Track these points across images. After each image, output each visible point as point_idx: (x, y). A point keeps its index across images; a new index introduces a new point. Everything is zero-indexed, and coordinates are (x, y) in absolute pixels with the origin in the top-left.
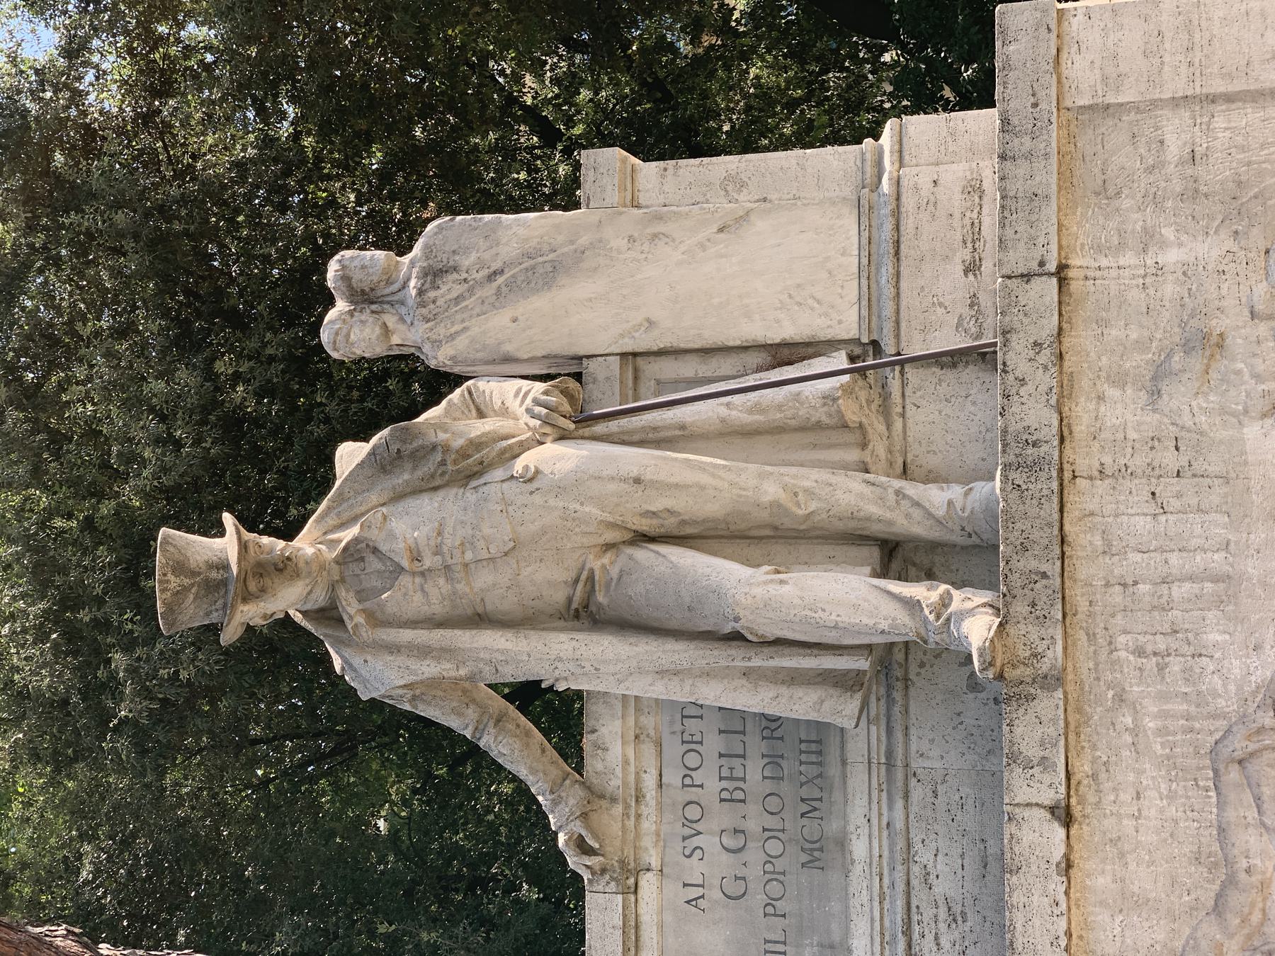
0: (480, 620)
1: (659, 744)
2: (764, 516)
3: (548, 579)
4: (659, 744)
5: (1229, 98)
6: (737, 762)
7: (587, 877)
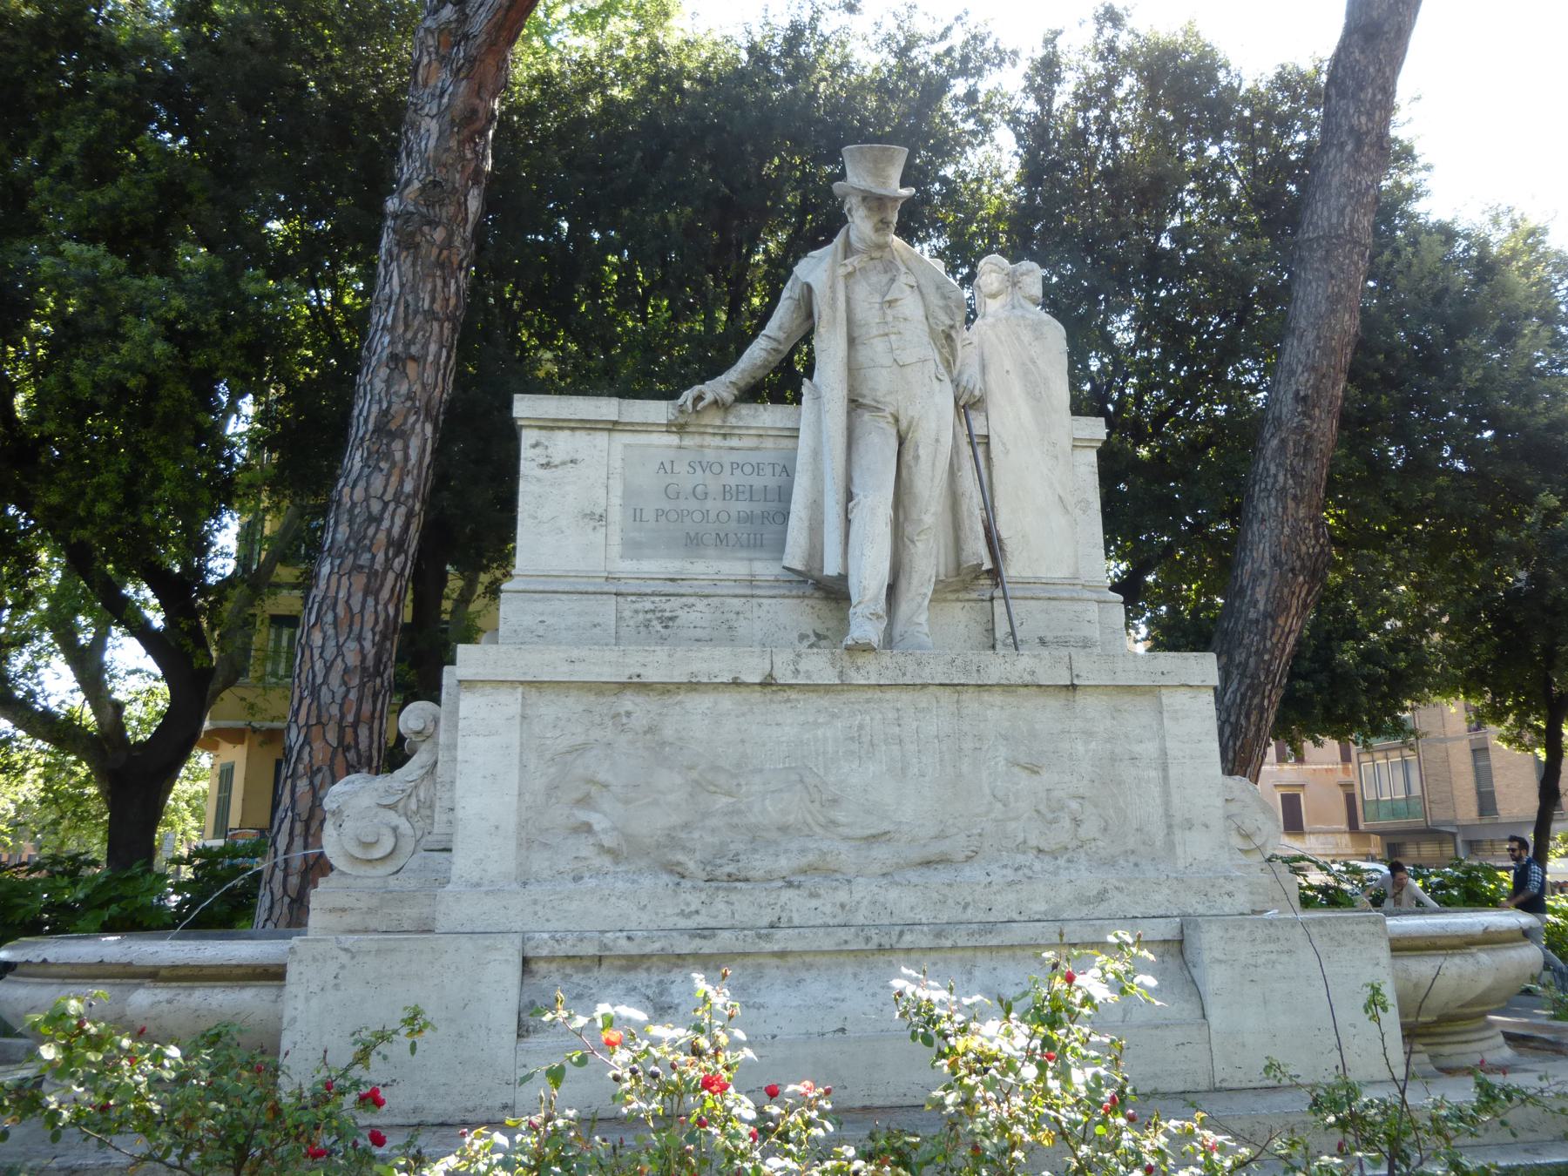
0: (852, 341)
1: (757, 449)
2: (915, 516)
3: (880, 382)
4: (757, 449)
5: (1166, 778)
6: (747, 495)
7: (680, 401)
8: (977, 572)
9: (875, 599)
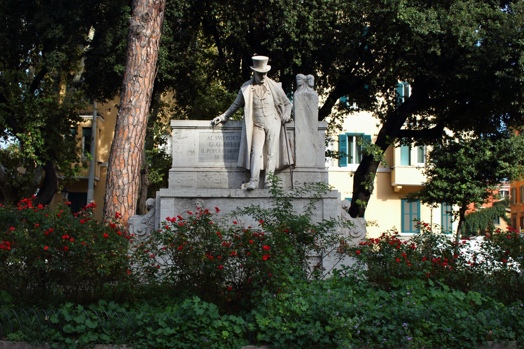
8: (287, 167)
9: (256, 177)
